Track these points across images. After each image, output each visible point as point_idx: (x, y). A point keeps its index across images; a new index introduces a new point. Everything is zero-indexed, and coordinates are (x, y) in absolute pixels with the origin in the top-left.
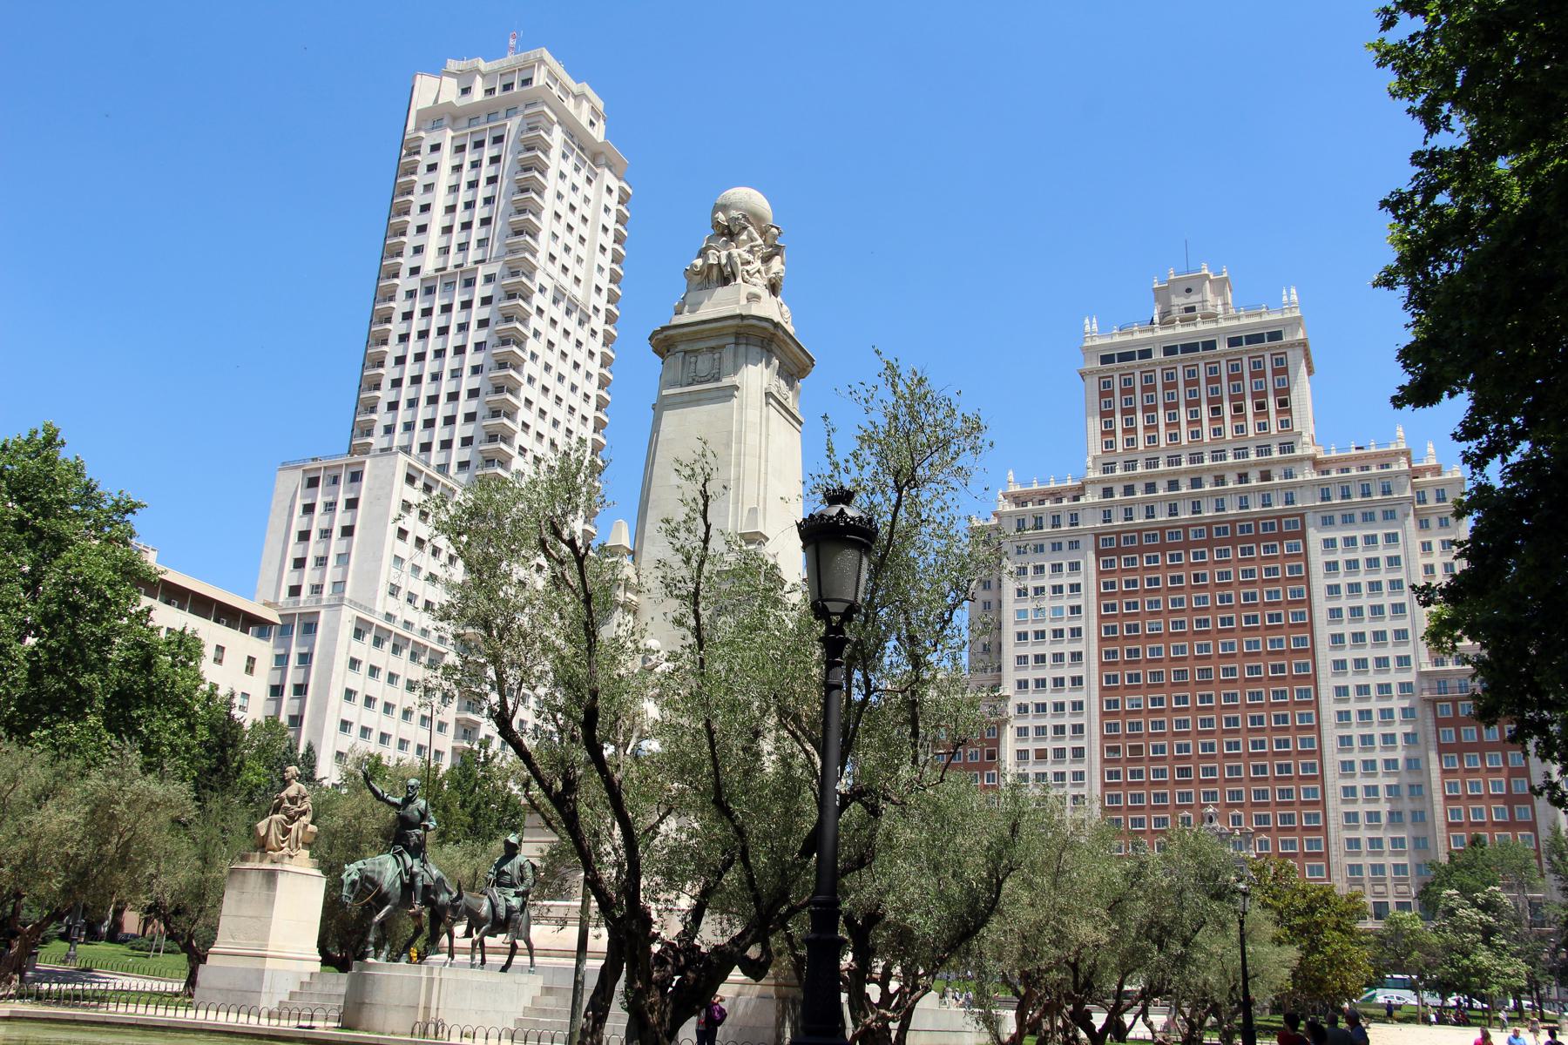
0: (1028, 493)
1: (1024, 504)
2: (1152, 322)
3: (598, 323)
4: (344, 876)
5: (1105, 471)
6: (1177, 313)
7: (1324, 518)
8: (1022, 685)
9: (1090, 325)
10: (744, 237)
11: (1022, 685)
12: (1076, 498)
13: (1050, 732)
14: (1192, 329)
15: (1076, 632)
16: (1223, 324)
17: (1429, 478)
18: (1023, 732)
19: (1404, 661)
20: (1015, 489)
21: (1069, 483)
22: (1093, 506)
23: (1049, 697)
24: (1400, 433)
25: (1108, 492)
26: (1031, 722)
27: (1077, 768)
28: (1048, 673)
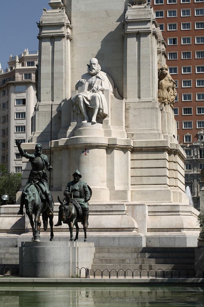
4: (27, 198)
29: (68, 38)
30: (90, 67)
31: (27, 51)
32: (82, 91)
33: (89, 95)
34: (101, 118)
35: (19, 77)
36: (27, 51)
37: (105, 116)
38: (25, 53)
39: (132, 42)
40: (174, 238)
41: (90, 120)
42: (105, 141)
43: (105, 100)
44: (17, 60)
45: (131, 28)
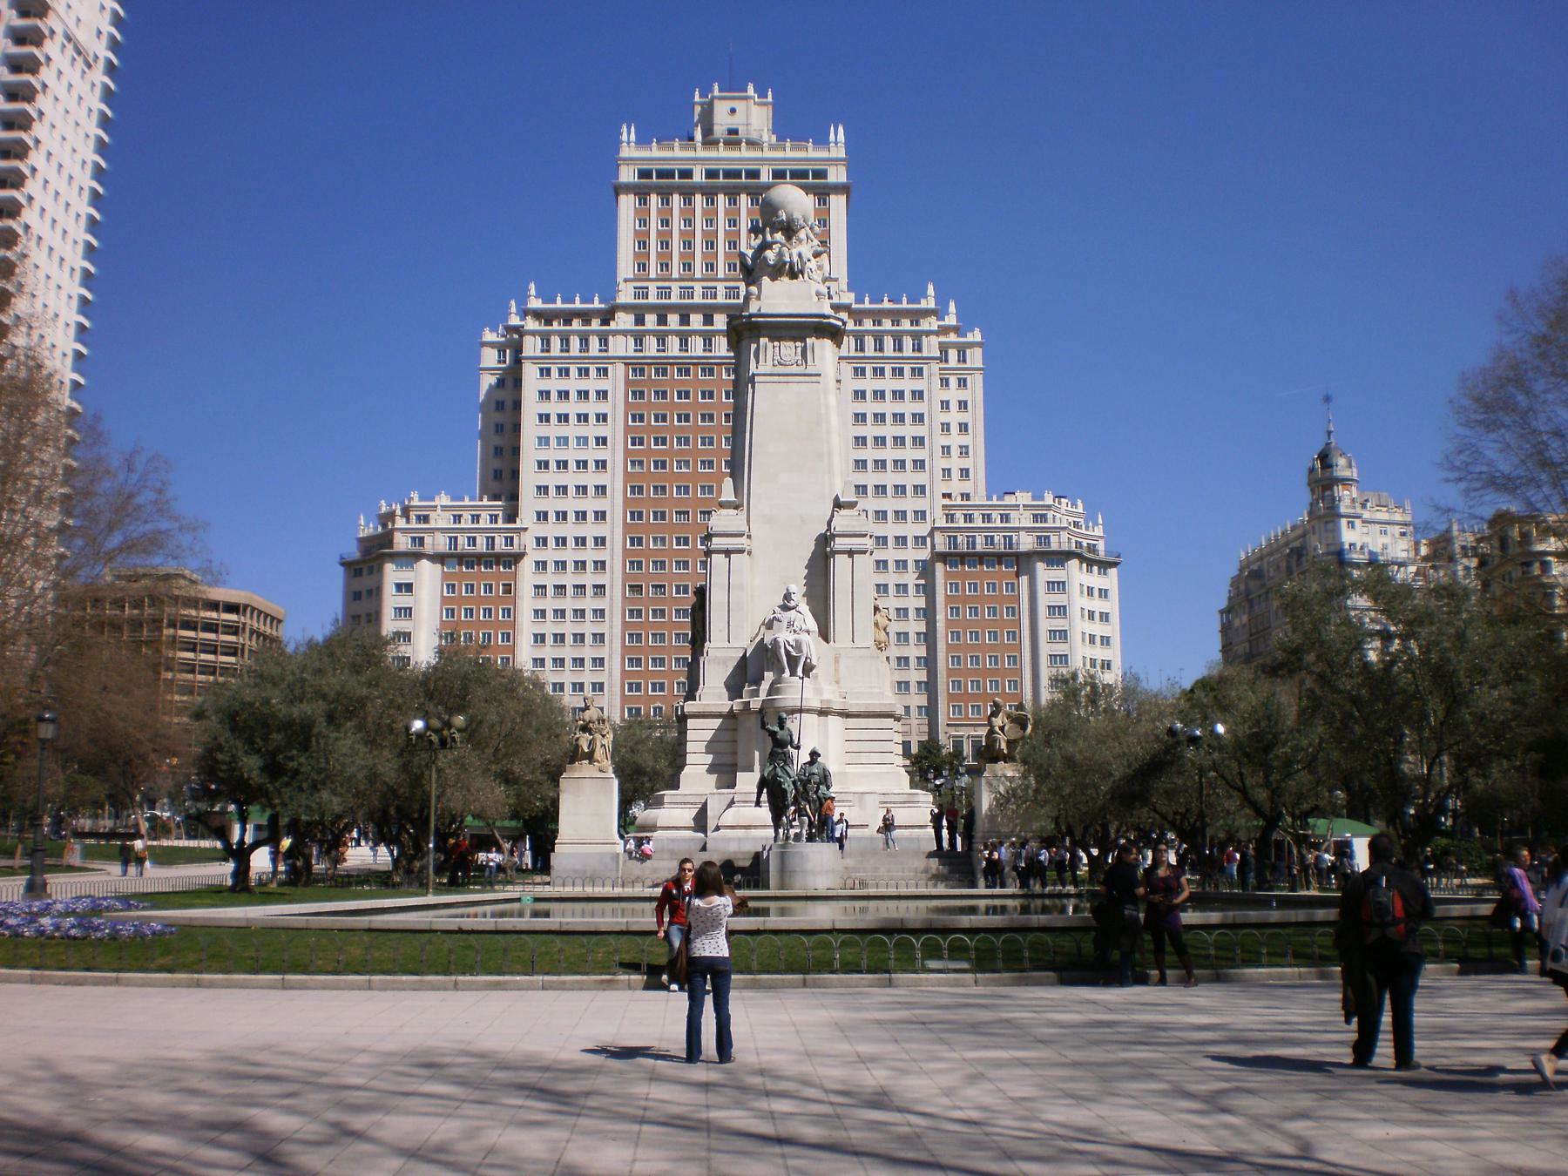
0: (551, 310)
1: (549, 322)
2: (691, 139)
3: (99, 76)
5: (637, 296)
6: (719, 131)
7: (856, 369)
8: (542, 516)
9: (628, 134)
10: (802, 234)
11: (542, 516)
12: (605, 322)
13: (570, 567)
14: (735, 154)
15: (601, 465)
16: (768, 154)
17: (953, 338)
18: (541, 566)
19: (920, 515)
20: (535, 303)
21: (597, 304)
22: (624, 333)
23: (570, 530)
24: (931, 290)
25: (640, 320)
26: (551, 554)
27: (599, 604)
28: (571, 504)
29: (749, 553)
30: (787, 597)
31: (415, 495)
32: (780, 630)
33: (791, 638)
34: (808, 669)
35: (402, 543)
36: (415, 495)
37: (812, 668)
38: (411, 499)
39: (841, 564)
40: (918, 839)
41: (793, 673)
42: (816, 704)
43: (813, 647)
44: (398, 512)
45: (840, 544)
